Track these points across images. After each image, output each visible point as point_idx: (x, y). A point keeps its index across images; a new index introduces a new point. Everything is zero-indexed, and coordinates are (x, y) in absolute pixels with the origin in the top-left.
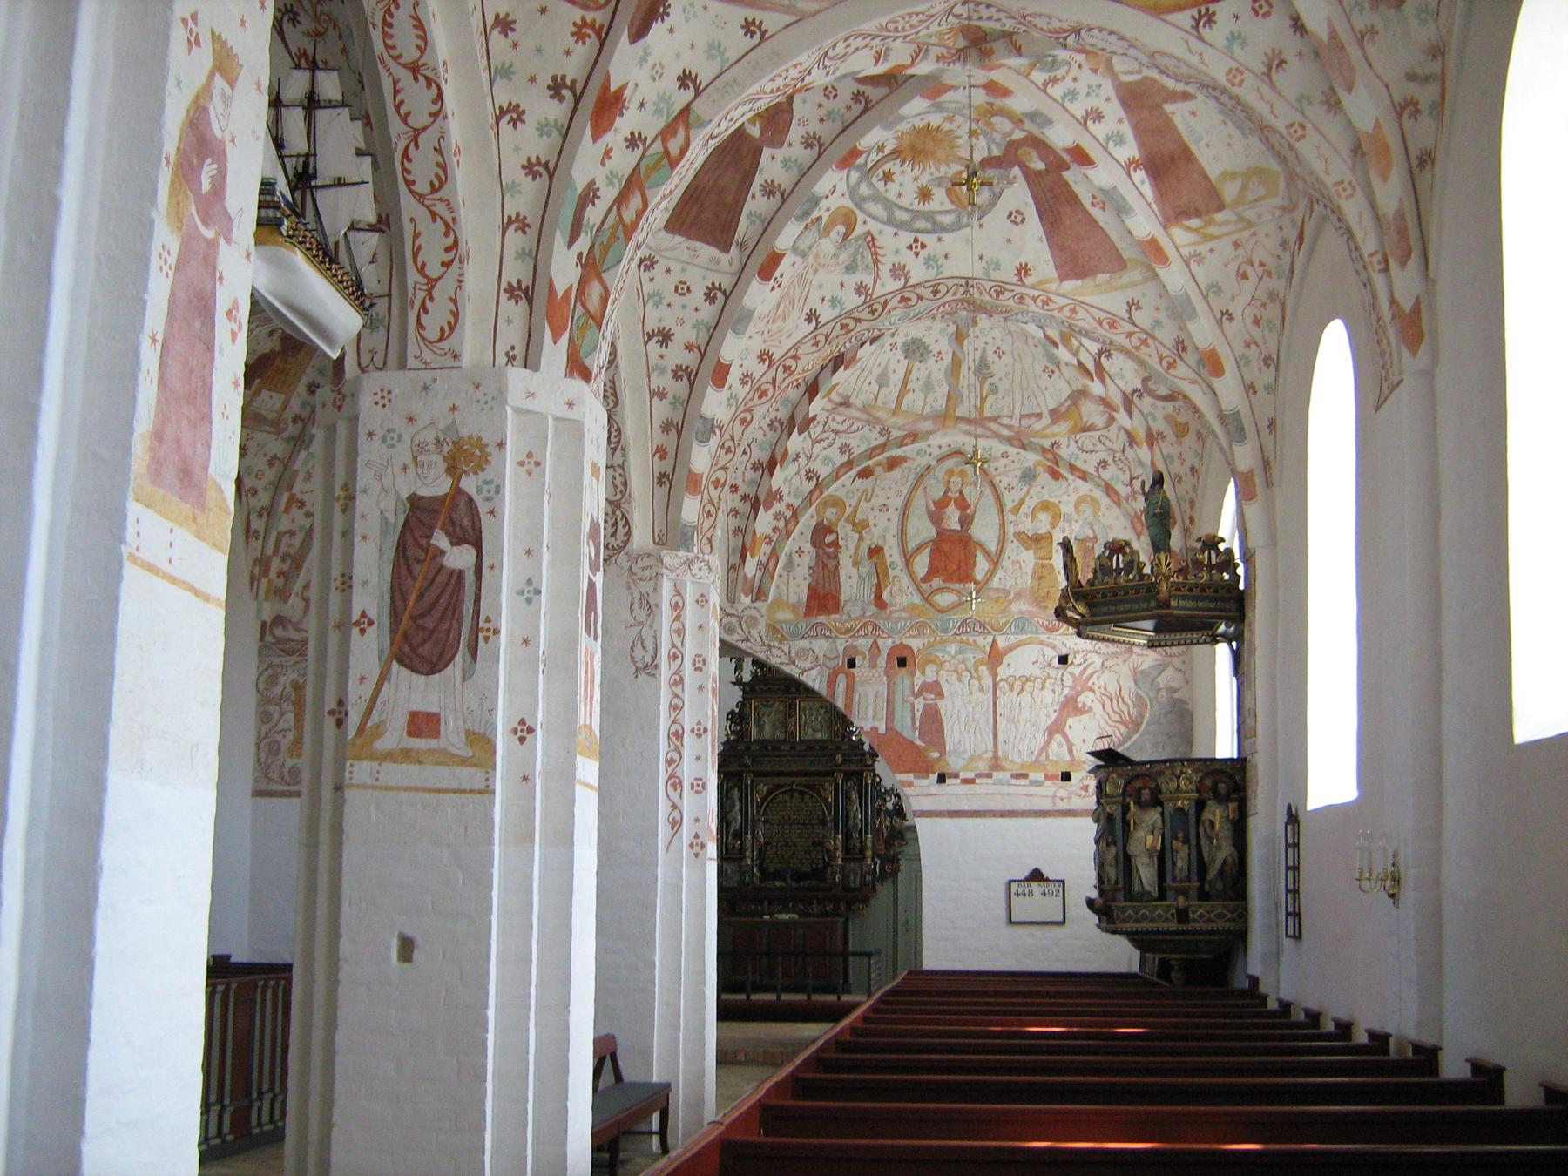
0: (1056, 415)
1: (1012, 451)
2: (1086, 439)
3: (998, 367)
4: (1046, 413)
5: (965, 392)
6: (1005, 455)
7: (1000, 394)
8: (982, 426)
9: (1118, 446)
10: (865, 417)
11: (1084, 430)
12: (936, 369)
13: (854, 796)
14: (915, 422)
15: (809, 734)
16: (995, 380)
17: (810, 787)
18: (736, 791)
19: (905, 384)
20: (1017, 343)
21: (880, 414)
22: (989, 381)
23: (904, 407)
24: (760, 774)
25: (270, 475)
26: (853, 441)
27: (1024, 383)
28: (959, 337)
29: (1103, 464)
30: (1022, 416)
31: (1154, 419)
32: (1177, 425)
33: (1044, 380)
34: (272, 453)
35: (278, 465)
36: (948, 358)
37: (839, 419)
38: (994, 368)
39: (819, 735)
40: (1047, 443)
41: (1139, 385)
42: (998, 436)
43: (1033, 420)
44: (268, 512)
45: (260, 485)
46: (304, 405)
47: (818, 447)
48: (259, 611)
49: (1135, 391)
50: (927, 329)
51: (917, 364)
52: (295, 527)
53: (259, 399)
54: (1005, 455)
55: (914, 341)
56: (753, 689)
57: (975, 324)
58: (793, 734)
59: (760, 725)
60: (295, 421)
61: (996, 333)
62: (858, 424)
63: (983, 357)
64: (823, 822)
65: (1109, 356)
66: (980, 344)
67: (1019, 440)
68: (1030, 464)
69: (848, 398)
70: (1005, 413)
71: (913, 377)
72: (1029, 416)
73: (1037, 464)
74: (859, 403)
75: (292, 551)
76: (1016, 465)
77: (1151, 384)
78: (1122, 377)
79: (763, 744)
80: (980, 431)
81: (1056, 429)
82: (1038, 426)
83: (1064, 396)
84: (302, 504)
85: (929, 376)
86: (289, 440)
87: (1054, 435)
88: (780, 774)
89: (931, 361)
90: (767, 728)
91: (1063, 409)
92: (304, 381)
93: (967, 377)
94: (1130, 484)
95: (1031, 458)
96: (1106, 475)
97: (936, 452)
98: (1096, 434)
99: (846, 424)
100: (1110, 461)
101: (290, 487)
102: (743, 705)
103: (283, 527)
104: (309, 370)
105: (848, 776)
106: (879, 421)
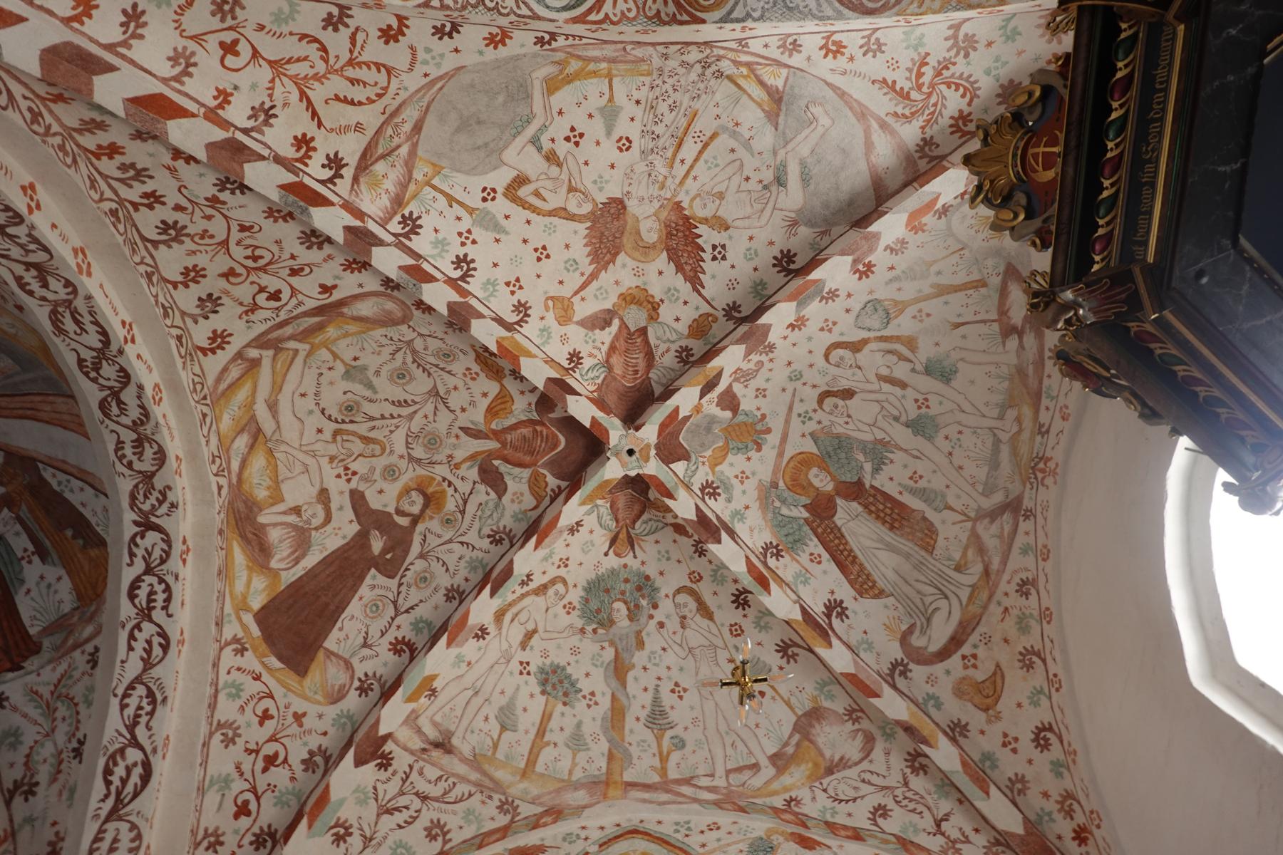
0: (780, 761)
1: (725, 818)
2: (841, 783)
3: (680, 713)
4: (764, 762)
5: (634, 750)
6: (714, 827)
7: (689, 748)
8: (668, 791)
9: (894, 779)
10: (474, 776)
11: (830, 771)
12: (591, 718)
14: (558, 791)
19: (541, 732)
21: (500, 774)
22: (669, 733)
23: (540, 768)
26: (452, 821)
27: (723, 728)
28: (619, 670)
29: (880, 811)
30: (728, 772)
31: (938, 706)
32: (978, 687)
36: (605, 703)
37: (432, 773)
38: (673, 716)
40: (778, 802)
41: (896, 652)
42: (696, 800)
43: (747, 773)
47: (388, 822)
49: (895, 665)
50: (575, 651)
51: (560, 708)
54: (714, 827)
55: (556, 669)
57: (641, 644)
61: (670, 658)
62: (462, 789)
63: (656, 700)
65: (843, 614)
67: (733, 802)
68: (759, 832)
69: (449, 735)
70: (701, 771)
71: (554, 724)
72: (739, 770)
73: (770, 832)
74: (466, 750)
76: (736, 837)
77: (917, 641)
78: (870, 646)
80: (664, 797)
81: (786, 780)
82: (757, 781)
83: (787, 729)
85: (579, 725)
87: (786, 789)
89: (581, 705)
91: (790, 750)
93: (636, 732)
94: (939, 831)
95: (759, 826)
96: (890, 826)
97: (596, 835)
98: (852, 773)
99: (443, 785)
100: (891, 805)
106: (498, 786)
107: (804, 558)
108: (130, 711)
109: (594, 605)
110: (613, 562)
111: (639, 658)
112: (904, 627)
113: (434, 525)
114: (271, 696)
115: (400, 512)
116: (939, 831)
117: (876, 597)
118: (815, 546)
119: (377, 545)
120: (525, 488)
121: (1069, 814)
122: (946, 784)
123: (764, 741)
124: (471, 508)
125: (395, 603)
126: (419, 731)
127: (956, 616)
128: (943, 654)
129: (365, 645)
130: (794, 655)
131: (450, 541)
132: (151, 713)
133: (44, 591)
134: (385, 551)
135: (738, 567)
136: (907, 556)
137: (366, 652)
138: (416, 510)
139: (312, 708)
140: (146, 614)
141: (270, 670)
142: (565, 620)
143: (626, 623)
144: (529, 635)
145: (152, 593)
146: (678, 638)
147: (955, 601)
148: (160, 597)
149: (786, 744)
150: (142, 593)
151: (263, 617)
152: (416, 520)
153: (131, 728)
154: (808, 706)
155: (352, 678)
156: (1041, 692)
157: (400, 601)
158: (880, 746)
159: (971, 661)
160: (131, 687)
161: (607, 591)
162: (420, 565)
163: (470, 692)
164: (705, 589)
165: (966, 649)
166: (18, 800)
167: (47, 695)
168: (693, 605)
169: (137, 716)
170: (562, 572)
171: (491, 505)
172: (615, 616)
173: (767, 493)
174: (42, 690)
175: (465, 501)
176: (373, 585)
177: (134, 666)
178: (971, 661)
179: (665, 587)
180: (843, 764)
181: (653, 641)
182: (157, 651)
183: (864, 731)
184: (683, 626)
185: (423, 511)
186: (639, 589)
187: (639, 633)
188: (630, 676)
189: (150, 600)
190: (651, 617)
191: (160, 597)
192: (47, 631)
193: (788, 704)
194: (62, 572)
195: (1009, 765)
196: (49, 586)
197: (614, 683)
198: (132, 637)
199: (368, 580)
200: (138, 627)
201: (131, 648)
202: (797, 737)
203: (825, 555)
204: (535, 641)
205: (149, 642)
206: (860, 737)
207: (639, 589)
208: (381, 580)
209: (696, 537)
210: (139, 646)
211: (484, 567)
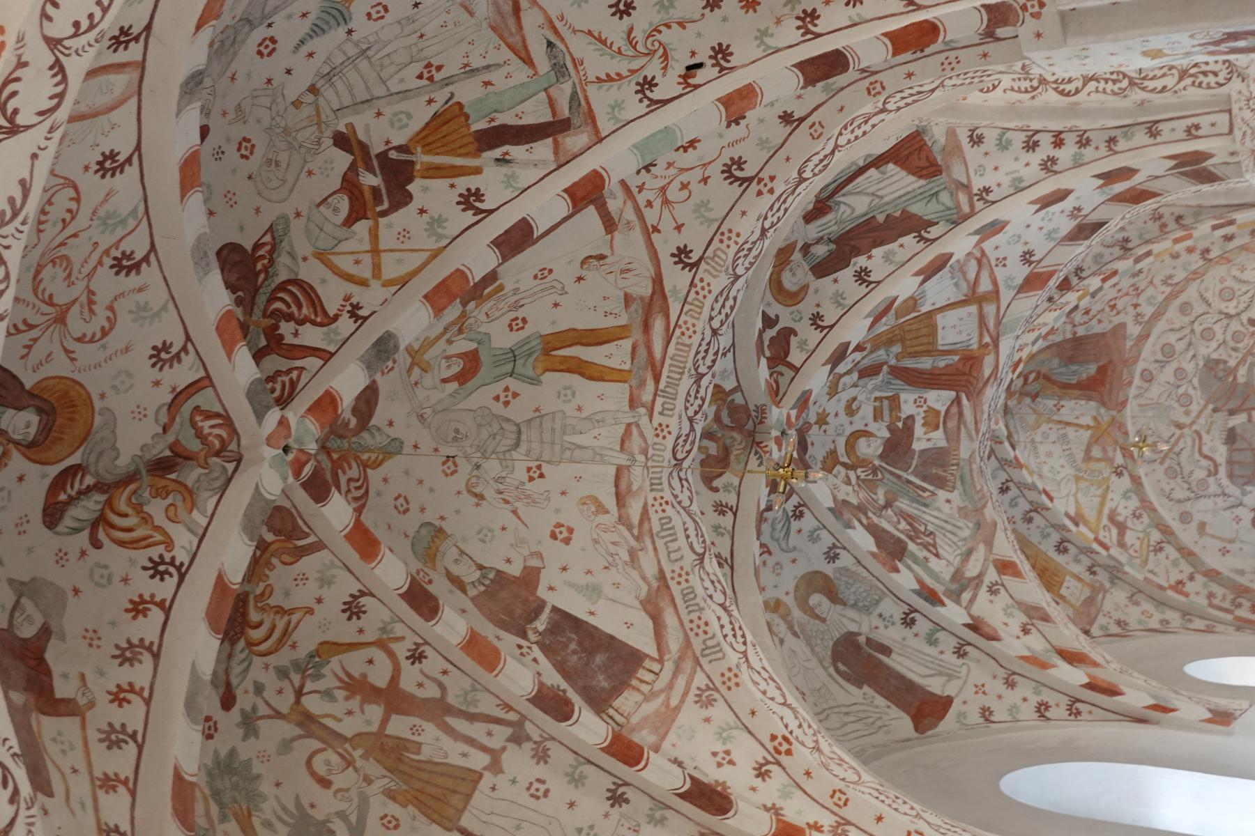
25: (1148, 606)
34: (1126, 602)
35: (1138, 597)
44: (1186, 614)
45: (1157, 616)
46: (1078, 561)
52: (1204, 592)
53: (1069, 598)
60: (1094, 573)
75: (1230, 597)
84: (1180, 582)
86: (1112, 582)
92: (1053, 554)
101: (1161, 587)
103: (1205, 602)
104: (1042, 547)
166: (1130, 245)
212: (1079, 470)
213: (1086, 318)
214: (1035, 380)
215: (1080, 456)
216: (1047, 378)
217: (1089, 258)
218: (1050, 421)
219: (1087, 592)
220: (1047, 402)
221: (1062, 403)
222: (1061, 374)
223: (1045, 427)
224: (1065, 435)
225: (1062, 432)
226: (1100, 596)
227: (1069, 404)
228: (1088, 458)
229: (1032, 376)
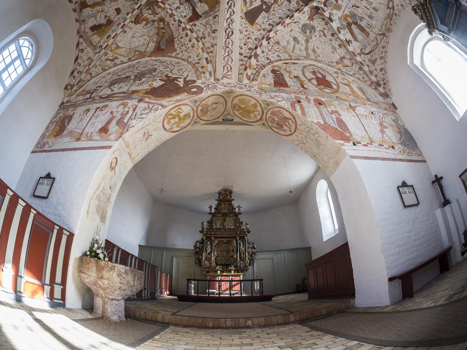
9: (357, 70)
11: (346, 66)
13: (241, 244)
15: (230, 227)
16: (318, 54)
17: (229, 241)
18: (209, 242)
20: (323, 46)
24: (217, 237)
27: (327, 56)
28: (307, 41)
32: (372, 61)
33: (332, 55)
39: (232, 227)
48: (64, 98)
50: (299, 36)
56: (214, 215)
57: (311, 38)
58: (225, 227)
59: (216, 225)
61: (316, 42)
63: (314, 48)
64: (233, 251)
66: (312, 44)
77: (363, 51)
79: (217, 229)
83: (338, 59)
88: (221, 237)
90: (218, 225)
91: (339, 62)
98: (350, 68)
100: (356, 73)
102: (211, 219)
105: (240, 237)
107: (346, 31)
108: (228, 23)
109: (303, 29)
110: (308, 22)
111: (311, 40)
112: (361, 48)
113: (276, 6)
114: (247, 27)
115: (269, 2)
116: (363, 79)
117: (357, 42)
118: (347, 30)
119: (264, 7)
120: (295, 3)
121: (383, 81)
122: (365, 73)
123: (334, 59)
124: (284, 4)
125: (268, 18)
126: (274, 40)
127: (371, 49)
128: (367, 54)
129: (263, 23)
130: (341, 47)
131: (279, 9)
132: (232, 23)
133: (202, 8)
134: (266, 8)
135: (335, 28)
136: (364, 37)
137: (263, 24)
138: (272, 2)
139: (255, 32)
140: (230, 7)
141: (247, 23)
142: (298, 30)
143: (309, 34)
144: (292, 30)
145: (231, 4)
146: (319, 39)
147: (371, 47)
148: (233, 5)
149: (338, 61)
150: (230, 4)
151: (245, 14)
152: (272, 4)
153: (229, 25)
154: (343, 56)
155: (261, 28)
156: (383, 63)
157: (269, 17)
158: (354, 65)
159: (372, 56)
160: (228, 19)
161: (306, 27)
162: (273, 12)
163: (282, 36)
164: (326, 32)
165: (371, 54)
167: (204, 24)
168: (322, 34)
169: (229, 24)
170: (299, 21)
171: (288, 5)
172: (307, 32)
173: (340, 18)
174: (203, 23)
175: (282, 3)
176: (263, 14)
177: (228, 16)
178: (372, 56)
179: (318, 29)
180: (348, 66)
181: (314, 38)
182: (232, 14)
183: (352, 63)
184: (320, 37)
185: (274, 3)
186: (312, 28)
187: (311, 36)
188: (309, 43)
189: (231, 5)
190: (314, 34)
191: (233, 5)
192: (203, 14)
193: (339, 55)
194: (205, 4)
195: (375, 73)
196: (203, 7)
197: (306, 43)
198: (227, 11)
199: (263, 13)
200: (229, 9)
201: (227, 13)
202: (340, 60)
203: (349, 32)
204: (292, 31)
205: (231, 12)
206: (351, 63)
207: (312, 28)
208: (265, 13)
209: (326, 21)
210: (229, 12)
211: (287, 15)
212: (133, 49)
213: (179, 39)
214: (163, 32)
215: (137, 49)
216: (163, 36)
217: (199, 28)
218: (150, 40)
219: (94, 44)
220: (156, 38)
221: (155, 43)
222: (164, 40)
223: (148, 39)
224: (144, 45)
225: (146, 44)
226: (92, 48)
227: (154, 45)
228: (136, 51)
229: (164, 31)
